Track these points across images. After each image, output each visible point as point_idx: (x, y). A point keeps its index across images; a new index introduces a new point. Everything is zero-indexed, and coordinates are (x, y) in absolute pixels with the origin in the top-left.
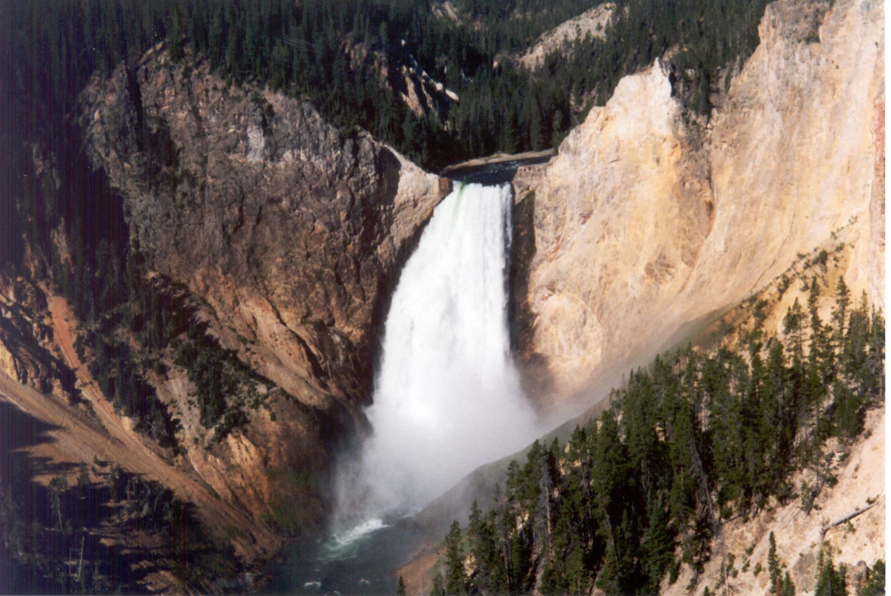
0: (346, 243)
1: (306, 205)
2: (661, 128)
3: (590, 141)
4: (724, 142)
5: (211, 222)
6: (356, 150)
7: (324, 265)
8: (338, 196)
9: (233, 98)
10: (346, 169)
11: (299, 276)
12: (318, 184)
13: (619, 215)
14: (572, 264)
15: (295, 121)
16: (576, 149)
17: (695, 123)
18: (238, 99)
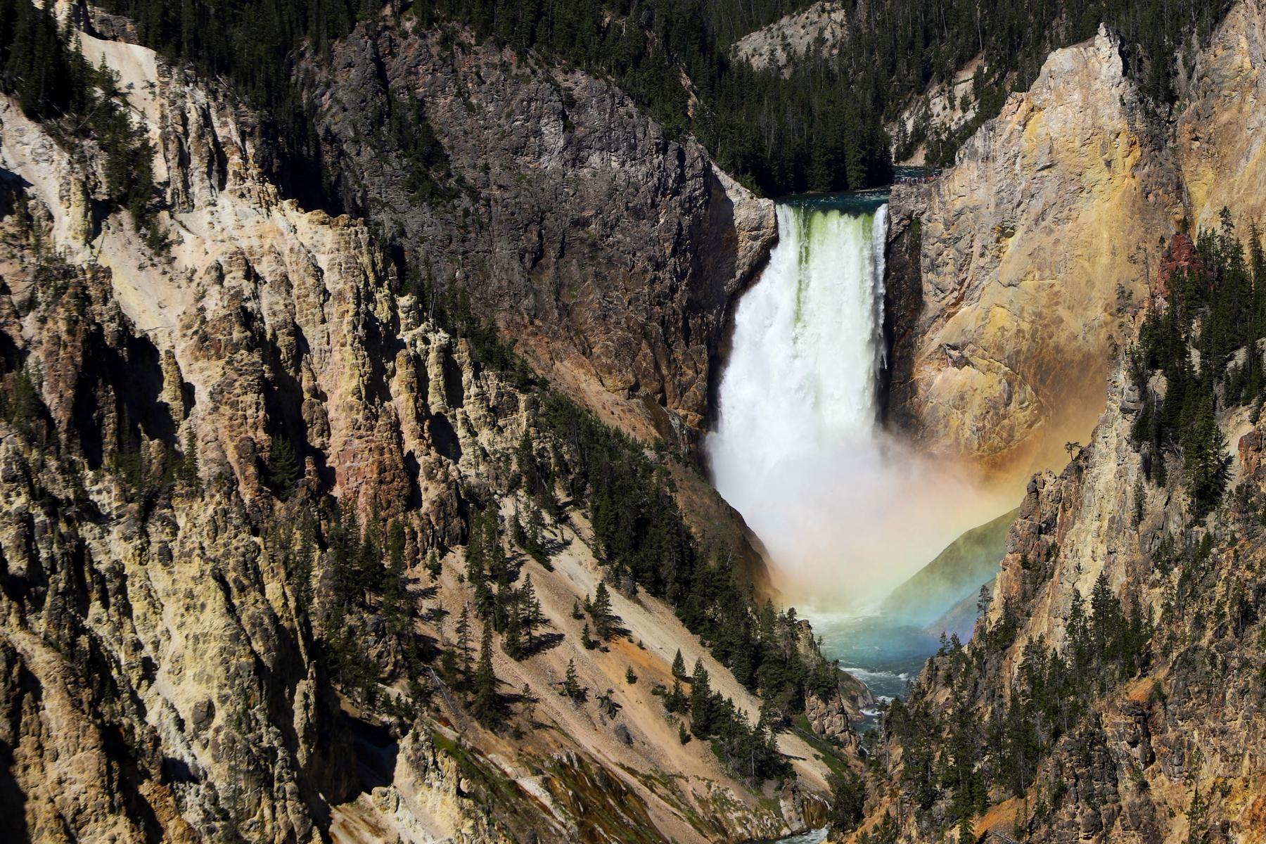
0: (673, 290)
1: (623, 230)
4: (1197, 139)
5: (502, 250)
6: (681, 156)
7: (649, 319)
8: (662, 221)
11: (622, 329)
12: (636, 200)
13: (1057, 241)
14: (983, 319)
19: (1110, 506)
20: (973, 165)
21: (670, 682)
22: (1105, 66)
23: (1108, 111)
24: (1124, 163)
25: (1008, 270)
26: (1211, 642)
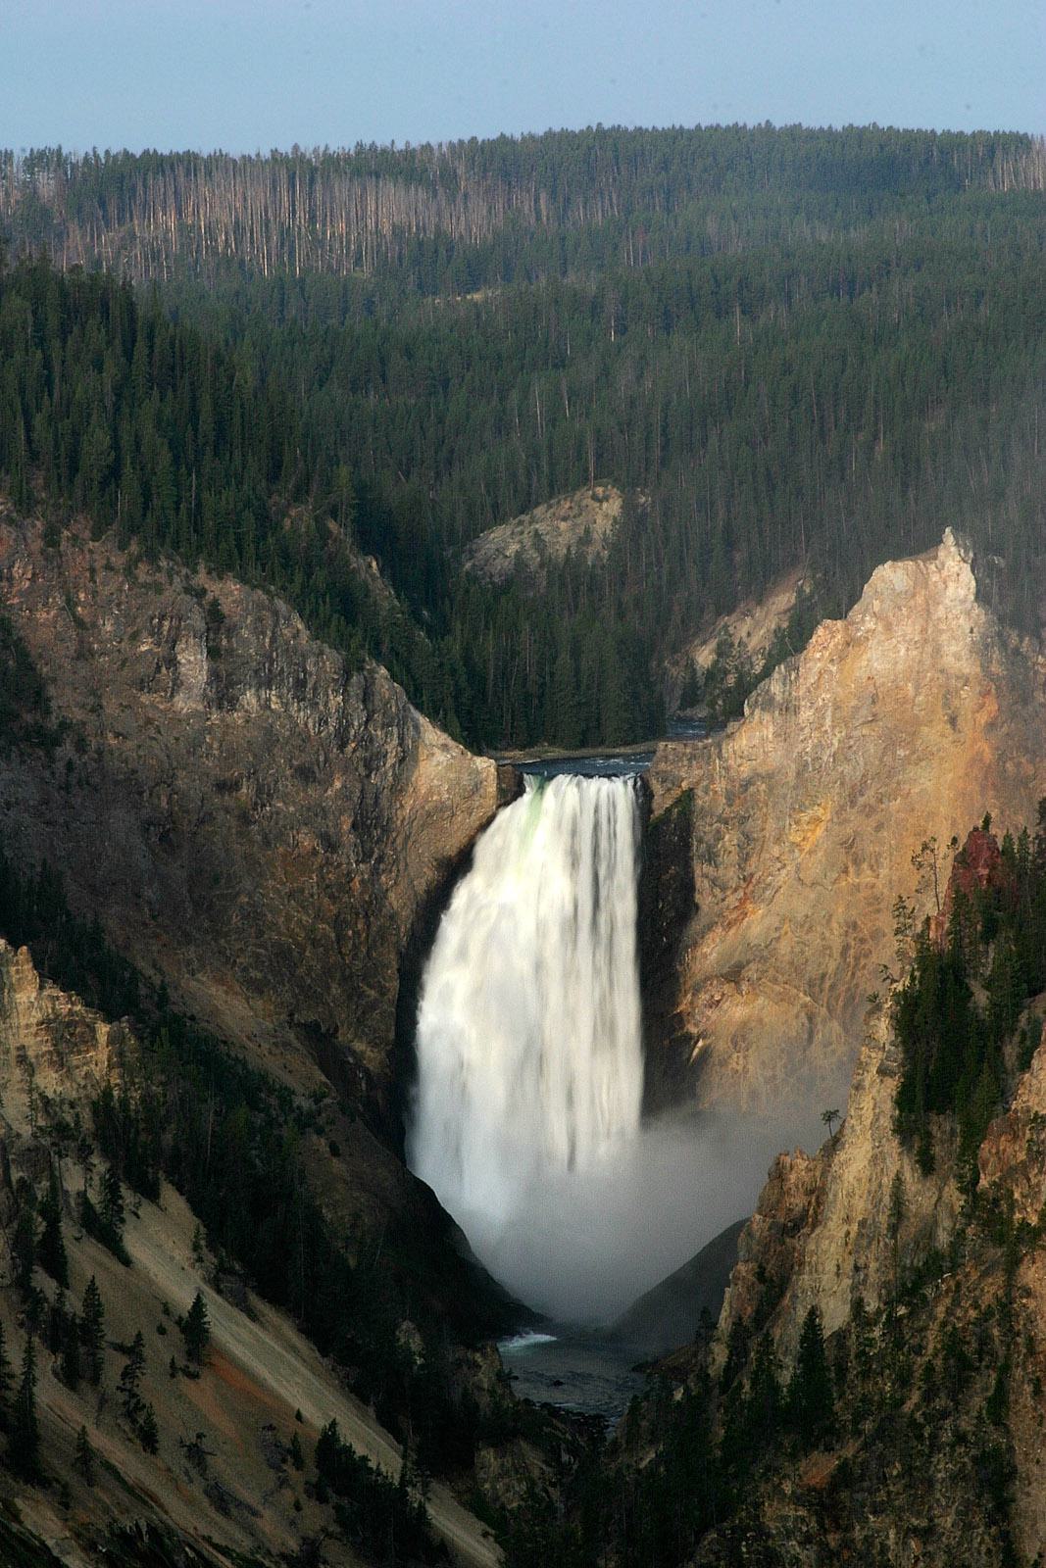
2: (958, 657)
3: (817, 685)
8: (338, 785)
9: (145, 585)
10: (352, 732)
11: (279, 934)
13: (879, 827)
15: (264, 634)
16: (788, 701)
17: (1017, 652)
20: (767, 717)
22: (952, 585)
23: (954, 649)
26: (917, 1406)
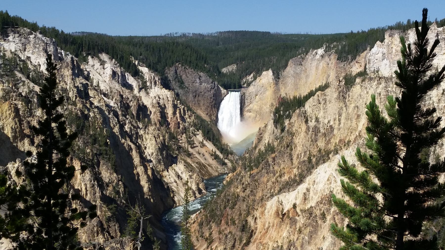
0: (213, 101)
5: (191, 95)
6: (214, 84)
18: (194, 73)
19: (270, 131)
21: (211, 152)
24: (272, 87)
25: (257, 100)
